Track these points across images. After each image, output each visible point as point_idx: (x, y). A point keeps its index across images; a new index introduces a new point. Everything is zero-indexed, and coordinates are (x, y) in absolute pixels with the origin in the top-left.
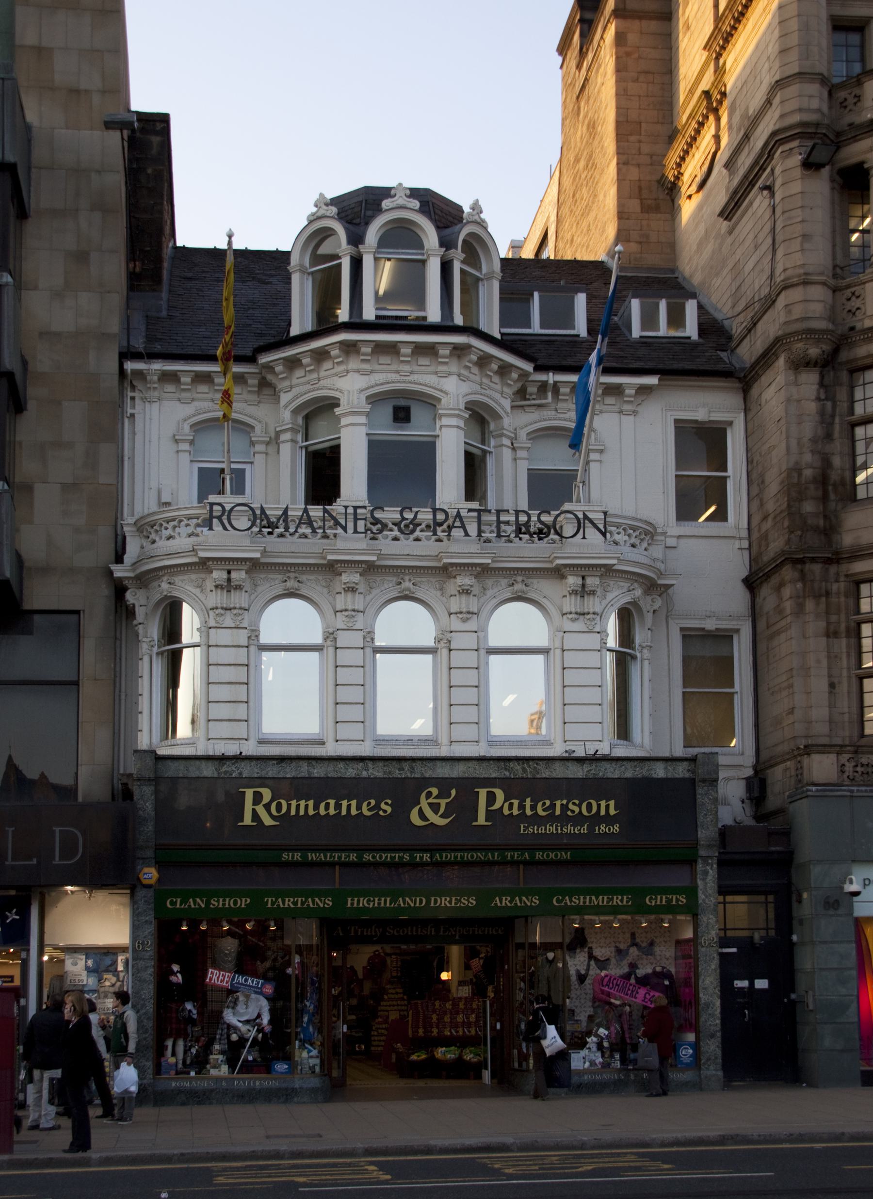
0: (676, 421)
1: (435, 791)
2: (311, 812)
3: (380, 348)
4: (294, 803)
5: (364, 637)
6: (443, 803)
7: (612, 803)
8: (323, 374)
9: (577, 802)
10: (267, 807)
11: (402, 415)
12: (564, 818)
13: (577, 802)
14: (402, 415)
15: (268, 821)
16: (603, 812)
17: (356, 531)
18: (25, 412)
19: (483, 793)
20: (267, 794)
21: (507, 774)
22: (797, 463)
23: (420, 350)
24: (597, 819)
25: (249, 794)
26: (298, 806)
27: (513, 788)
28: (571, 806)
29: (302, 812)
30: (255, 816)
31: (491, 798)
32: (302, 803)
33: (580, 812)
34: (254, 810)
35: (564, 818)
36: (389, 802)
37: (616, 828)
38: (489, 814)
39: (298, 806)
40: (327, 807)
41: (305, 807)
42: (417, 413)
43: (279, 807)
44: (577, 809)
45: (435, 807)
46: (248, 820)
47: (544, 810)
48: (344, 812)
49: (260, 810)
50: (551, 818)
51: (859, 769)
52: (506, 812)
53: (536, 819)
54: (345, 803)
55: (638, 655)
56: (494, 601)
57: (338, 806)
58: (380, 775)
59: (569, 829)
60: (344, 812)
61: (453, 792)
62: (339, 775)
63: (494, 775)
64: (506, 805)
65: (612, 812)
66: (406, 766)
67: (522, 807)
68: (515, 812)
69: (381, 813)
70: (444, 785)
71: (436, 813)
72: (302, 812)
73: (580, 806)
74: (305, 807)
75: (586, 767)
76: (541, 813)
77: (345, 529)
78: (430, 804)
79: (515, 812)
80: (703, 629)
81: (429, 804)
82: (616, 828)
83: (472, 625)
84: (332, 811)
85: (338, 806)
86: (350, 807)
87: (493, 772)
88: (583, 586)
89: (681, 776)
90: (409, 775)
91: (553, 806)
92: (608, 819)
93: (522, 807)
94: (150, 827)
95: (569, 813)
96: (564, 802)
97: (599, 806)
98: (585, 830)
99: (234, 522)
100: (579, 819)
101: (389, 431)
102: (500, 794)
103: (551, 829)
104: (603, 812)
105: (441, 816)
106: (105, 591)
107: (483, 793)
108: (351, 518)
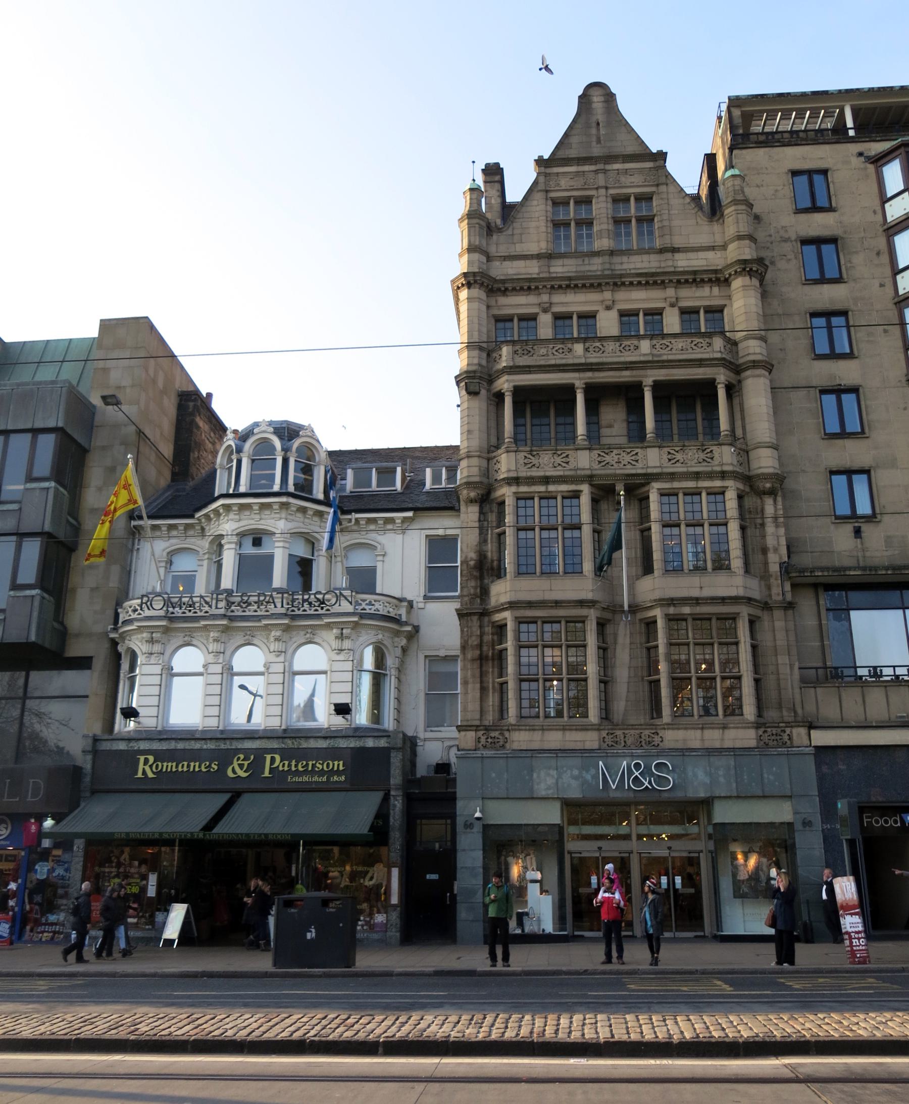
0: (427, 536)
1: (242, 756)
2: (174, 769)
3: (242, 507)
4: (165, 764)
5: (223, 668)
6: (246, 763)
7: (341, 763)
8: (221, 522)
9: (321, 762)
10: (151, 766)
11: (257, 542)
12: (313, 772)
13: (321, 762)
14: (257, 542)
15: (150, 775)
16: (336, 768)
17: (217, 608)
18: (77, 552)
19: (268, 757)
20: (151, 759)
21: (283, 746)
22: (466, 557)
23: (263, 506)
24: (332, 772)
25: (142, 758)
26: (167, 766)
27: (286, 755)
28: (318, 765)
29: (169, 770)
30: (144, 772)
31: (273, 760)
32: (170, 764)
33: (323, 769)
34: (144, 769)
35: (313, 772)
36: (217, 763)
37: (343, 778)
38: (272, 770)
39: (167, 766)
40: (183, 765)
41: (169, 766)
42: (265, 539)
43: (157, 766)
44: (320, 767)
45: (241, 766)
46: (140, 775)
47: (302, 767)
48: (192, 769)
49: (147, 768)
50: (306, 772)
51: (489, 740)
52: (281, 768)
53: (297, 773)
54: (192, 764)
55: (388, 672)
56: (295, 645)
57: (188, 766)
58: (213, 747)
59: (316, 779)
60: (192, 769)
61: (252, 757)
62: (191, 747)
63: (276, 746)
64: (282, 764)
65: (341, 768)
66: (228, 742)
67: (289, 765)
68: (286, 768)
69: (212, 770)
70: (247, 752)
71: (242, 769)
72: (169, 770)
73: (322, 764)
74: (169, 766)
75: (328, 741)
76: (300, 769)
77: (210, 606)
78: (239, 765)
79: (286, 768)
80: (438, 656)
81: (239, 765)
82: (343, 778)
83: (281, 659)
84: (185, 769)
85: (188, 766)
86: (195, 766)
87: (275, 745)
88: (342, 634)
89: (383, 746)
90: (229, 747)
91: (307, 765)
92: (339, 773)
93: (289, 765)
94: (88, 779)
95: (316, 769)
96: (314, 762)
97: (334, 764)
98: (325, 779)
99: (154, 606)
100: (322, 773)
101: (249, 549)
102: (278, 758)
103: (306, 779)
104: (336, 768)
105: (245, 772)
106: (106, 645)
107: (268, 757)
108: (214, 602)
